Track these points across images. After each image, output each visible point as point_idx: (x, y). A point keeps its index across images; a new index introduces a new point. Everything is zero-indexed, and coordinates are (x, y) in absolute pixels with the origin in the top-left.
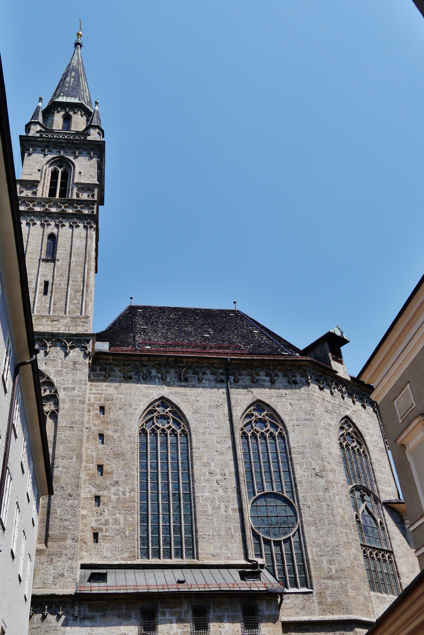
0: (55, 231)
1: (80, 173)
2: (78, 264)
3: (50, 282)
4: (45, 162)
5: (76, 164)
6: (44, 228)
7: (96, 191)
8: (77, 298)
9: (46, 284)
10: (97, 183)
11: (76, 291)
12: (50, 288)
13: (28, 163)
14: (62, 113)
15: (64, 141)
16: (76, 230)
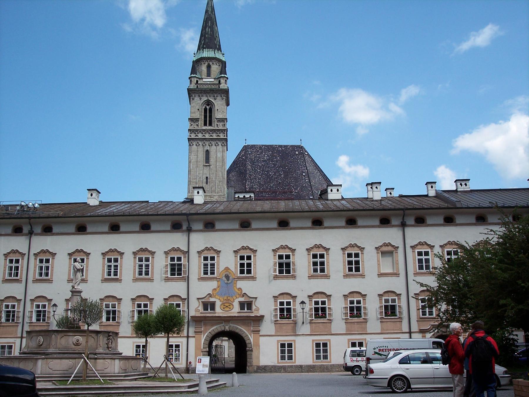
0: (208, 149)
1: (218, 110)
2: (220, 167)
3: (209, 177)
4: (200, 104)
5: (215, 104)
6: (203, 147)
8: (220, 185)
9: (207, 178)
11: (219, 182)
14: (206, 64)
15: (209, 90)
16: (218, 147)
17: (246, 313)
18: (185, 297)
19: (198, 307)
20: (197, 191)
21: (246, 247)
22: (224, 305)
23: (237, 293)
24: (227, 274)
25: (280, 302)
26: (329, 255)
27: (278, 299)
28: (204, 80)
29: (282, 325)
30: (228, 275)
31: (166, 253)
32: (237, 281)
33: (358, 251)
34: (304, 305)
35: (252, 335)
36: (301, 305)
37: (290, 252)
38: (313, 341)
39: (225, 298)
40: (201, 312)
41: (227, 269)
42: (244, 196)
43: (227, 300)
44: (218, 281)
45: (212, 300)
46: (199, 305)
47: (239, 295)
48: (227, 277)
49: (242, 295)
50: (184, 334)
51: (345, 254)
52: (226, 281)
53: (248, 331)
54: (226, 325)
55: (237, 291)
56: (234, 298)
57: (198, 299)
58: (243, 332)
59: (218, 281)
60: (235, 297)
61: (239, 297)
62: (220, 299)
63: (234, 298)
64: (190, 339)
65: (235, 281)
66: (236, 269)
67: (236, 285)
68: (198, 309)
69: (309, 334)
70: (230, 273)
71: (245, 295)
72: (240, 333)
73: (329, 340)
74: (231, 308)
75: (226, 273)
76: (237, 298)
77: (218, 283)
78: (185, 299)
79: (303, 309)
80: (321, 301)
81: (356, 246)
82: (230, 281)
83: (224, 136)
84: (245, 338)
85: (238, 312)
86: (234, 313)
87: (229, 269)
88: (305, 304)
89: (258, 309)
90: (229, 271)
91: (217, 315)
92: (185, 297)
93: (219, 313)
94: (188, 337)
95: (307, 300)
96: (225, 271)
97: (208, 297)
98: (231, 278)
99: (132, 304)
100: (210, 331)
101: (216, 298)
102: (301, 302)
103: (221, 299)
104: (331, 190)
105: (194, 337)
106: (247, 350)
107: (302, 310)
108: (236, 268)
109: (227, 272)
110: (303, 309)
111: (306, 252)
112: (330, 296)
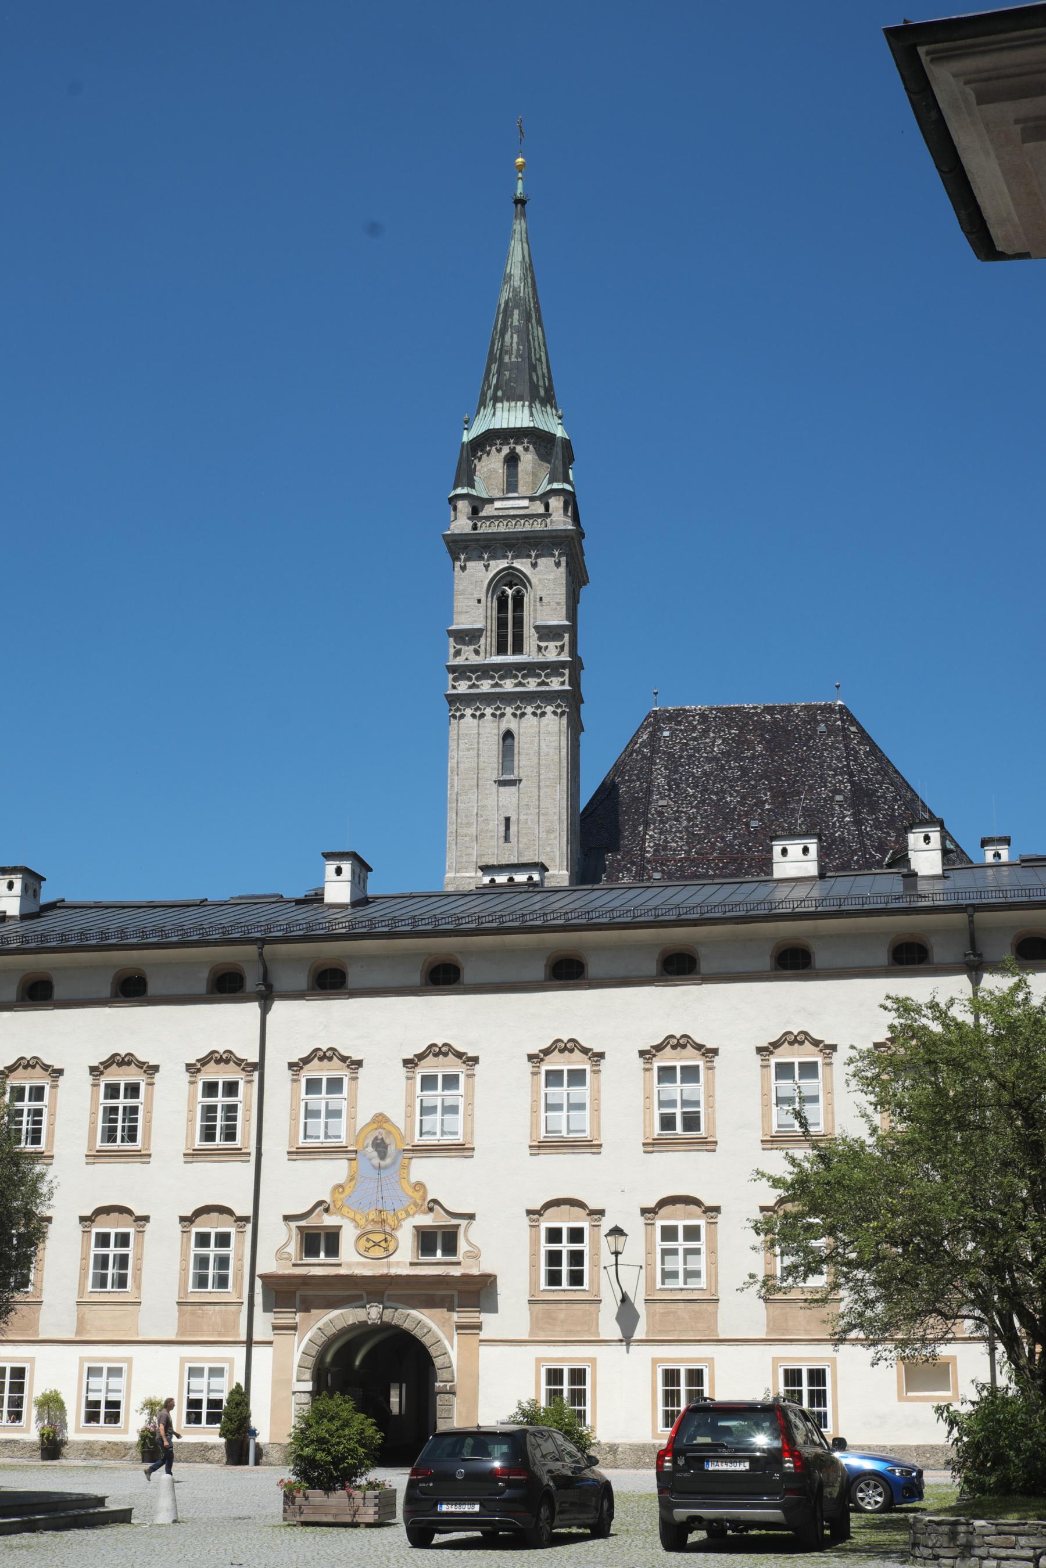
1: (541, 599)
3: (513, 819)
5: (533, 581)
7: (567, 636)
10: (567, 623)
12: (513, 829)
13: (461, 587)
17: (437, 1265)
18: (249, 1212)
19: (286, 1245)
20: (335, 866)
21: (443, 1049)
22: (368, 1240)
23: (411, 1200)
24: (380, 1137)
25: (663, 1228)
26: (716, 1070)
27: (542, 1218)
28: (498, 504)
29: (553, 1306)
30: (382, 1139)
31: (192, 1069)
32: (411, 1158)
33: (813, 1055)
34: (622, 1239)
35: (456, 1337)
36: (611, 1239)
37: (583, 1063)
38: (655, 1361)
39: (371, 1217)
40: (293, 1261)
41: (380, 1119)
42: (511, 879)
43: (377, 1222)
44: (350, 1160)
45: (329, 1220)
46: (290, 1237)
47: (415, 1204)
48: (380, 1147)
49: (425, 1206)
50: (238, 1335)
51: (768, 1066)
52: (376, 1161)
53: (442, 1325)
54: (371, 1307)
55: (411, 1194)
56: (399, 1214)
57: (287, 1218)
58: (425, 1331)
59: (350, 1160)
60: (403, 1212)
61: (415, 1213)
62: (353, 1220)
63: (400, 1217)
64: (256, 1350)
65: (406, 1161)
66: (408, 1120)
67: (408, 1174)
68: (285, 1250)
69: (644, 1338)
70: (389, 1133)
71: (436, 1207)
72: (417, 1333)
73: (710, 1361)
74: (391, 1249)
75: (376, 1133)
76: (408, 1215)
77: (350, 1166)
78: (246, 1219)
79: (617, 1254)
80: (686, 1228)
81: (806, 1038)
82: (388, 1161)
83: (563, 683)
84: (433, 1351)
85: (412, 1264)
86: (398, 1264)
87: (387, 1120)
88: (624, 1237)
89: (475, 1255)
90: (385, 1125)
91: (342, 1271)
92: (249, 1212)
93: (349, 1265)
94: (249, 1343)
95: (633, 1225)
96: (375, 1126)
97: (317, 1214)
98: (391, 1149)
99: (81, 1233)
100: (320, 1324)
101: (343, 1216)
102: (610, 1231)
103: (358, 1217)
104: (784, 852)
105: (270, 1343)
106: (436, 1390)
107: (614, 1256)
108: (409, 1116)
109: (381, 1130)
110: (617, 1254)
111: (640, 1062)
112: (717, 1209)
